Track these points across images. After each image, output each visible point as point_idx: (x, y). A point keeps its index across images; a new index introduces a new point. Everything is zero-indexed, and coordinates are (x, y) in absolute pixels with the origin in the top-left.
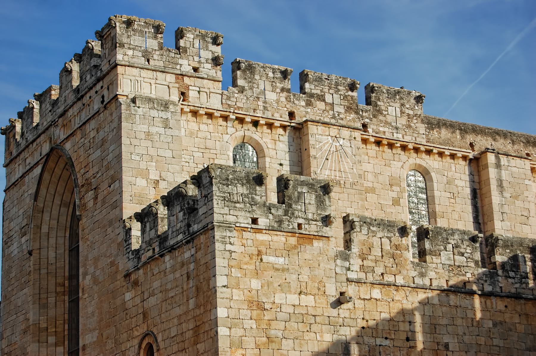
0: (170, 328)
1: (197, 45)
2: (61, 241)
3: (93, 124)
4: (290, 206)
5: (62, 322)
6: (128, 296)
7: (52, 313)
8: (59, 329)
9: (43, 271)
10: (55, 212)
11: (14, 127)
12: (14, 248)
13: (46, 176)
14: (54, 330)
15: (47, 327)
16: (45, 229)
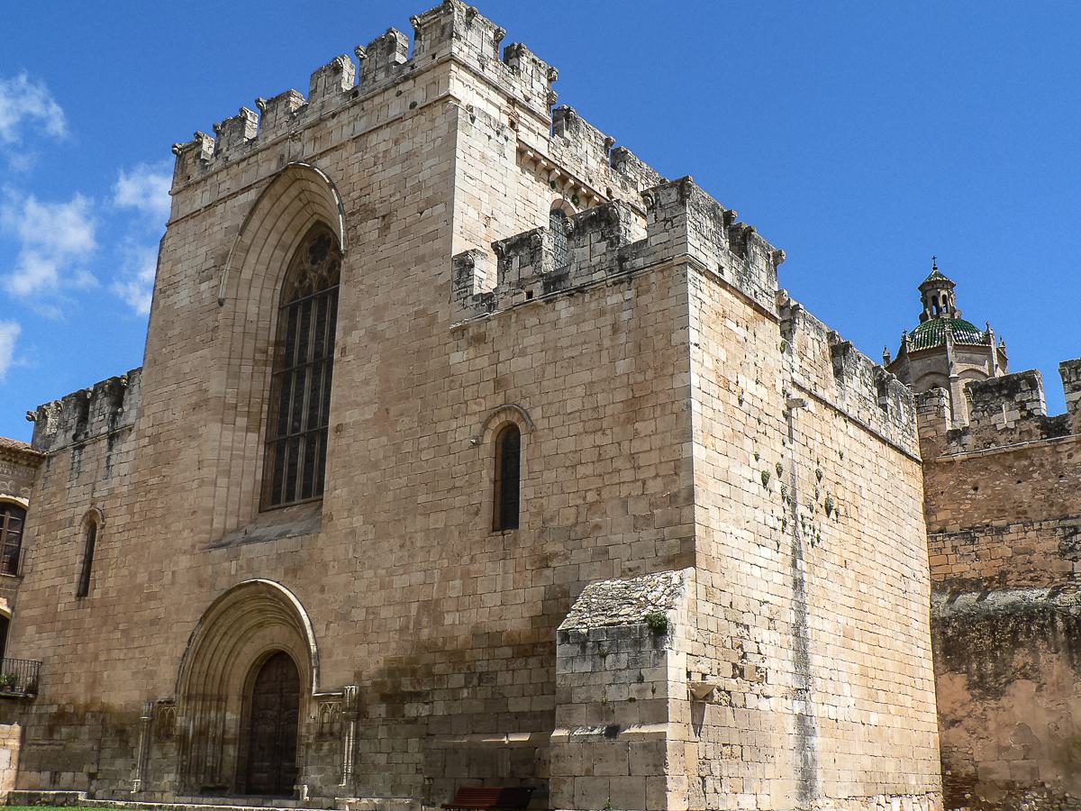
0: (655, 378)
1: (529, 72)
2: (268, 294)
3: (386, 134)
4: (747, 264)
6: (456, 358)
7: (245, 386)
8: (255, 409)
9: (238, 329)
10: (266, 255)
11: (200, 144)
12: (183, 298)
13: (266, 204)
14: (247, 409)
15: (236, 404)
16: (247, 274)
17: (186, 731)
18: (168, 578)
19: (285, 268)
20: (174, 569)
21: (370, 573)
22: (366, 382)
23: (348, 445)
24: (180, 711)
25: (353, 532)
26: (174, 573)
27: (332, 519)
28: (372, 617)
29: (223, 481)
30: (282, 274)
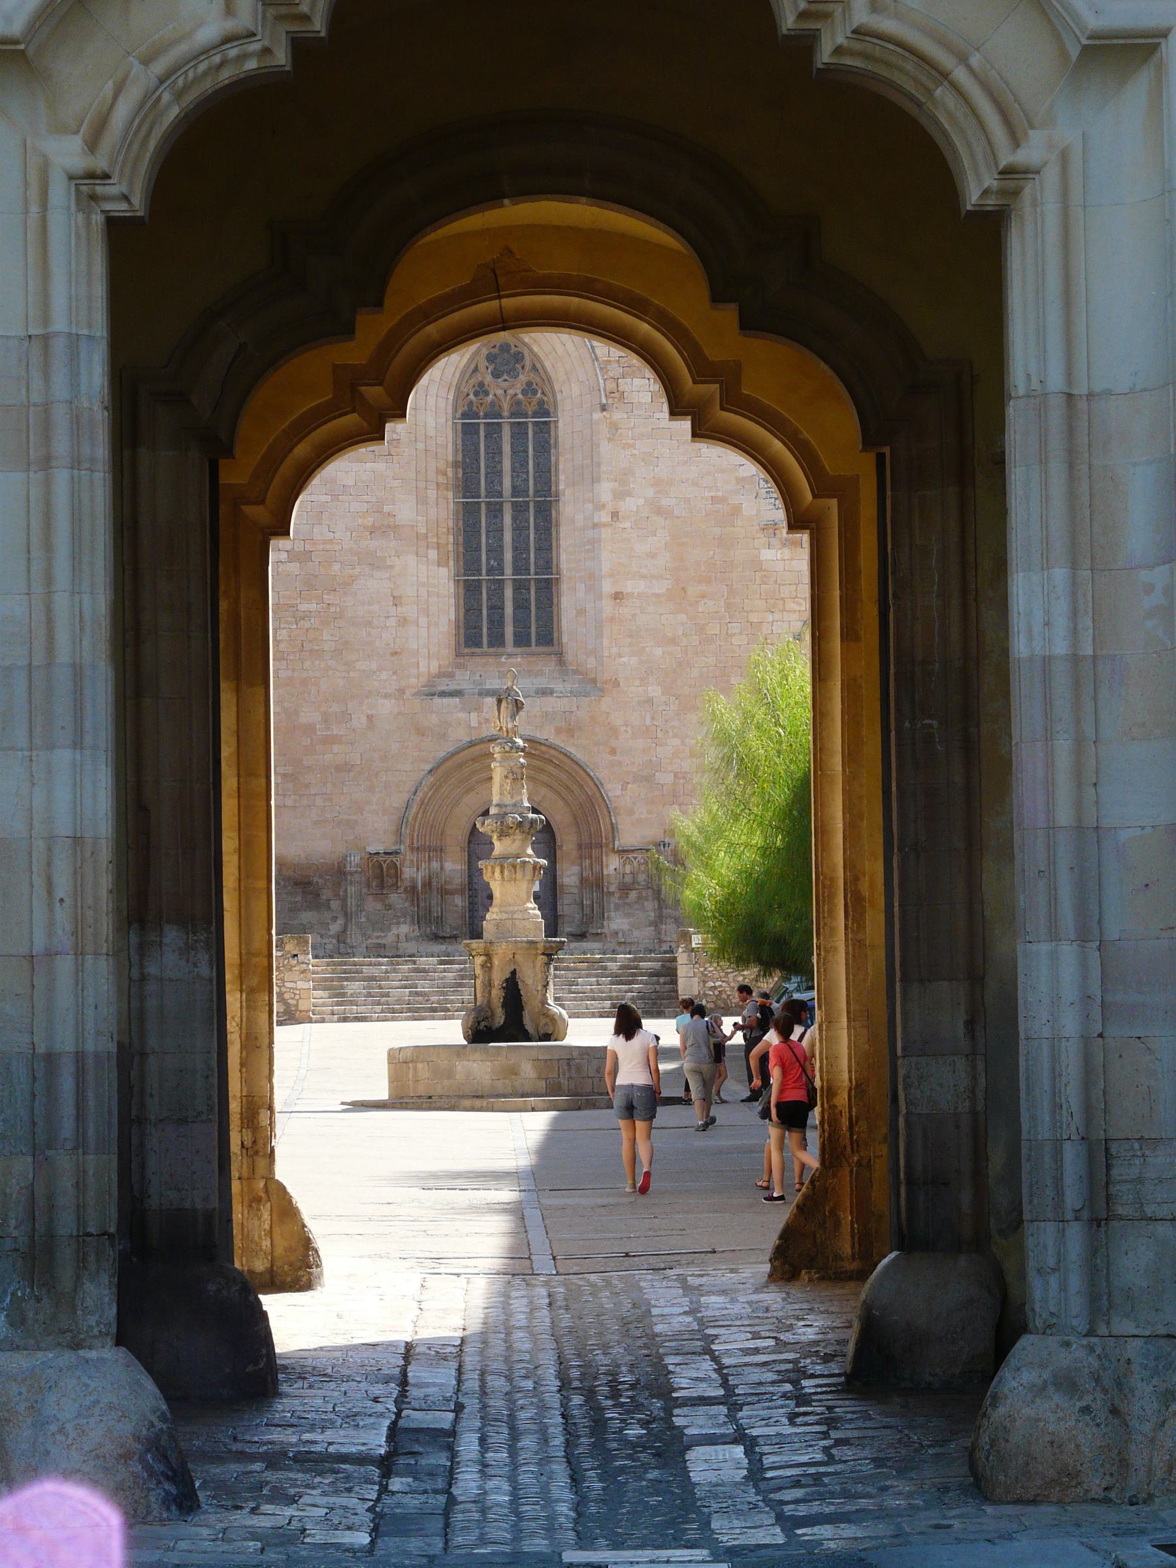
2: (442, 404)
5: (445, 530)
6: (767, 555)
17: (413, 880)
18: (359, 721)
19: (457, 375)
20: (370, 712)
21: (677, 742)
22: (652, 556)
23: (634, 615)
24: (407, 863)
25: (650, 701)
26: (370, 718)
27: (619, 685)
28: (681, 781)
29: (423, 621)
30: (454, 383)
